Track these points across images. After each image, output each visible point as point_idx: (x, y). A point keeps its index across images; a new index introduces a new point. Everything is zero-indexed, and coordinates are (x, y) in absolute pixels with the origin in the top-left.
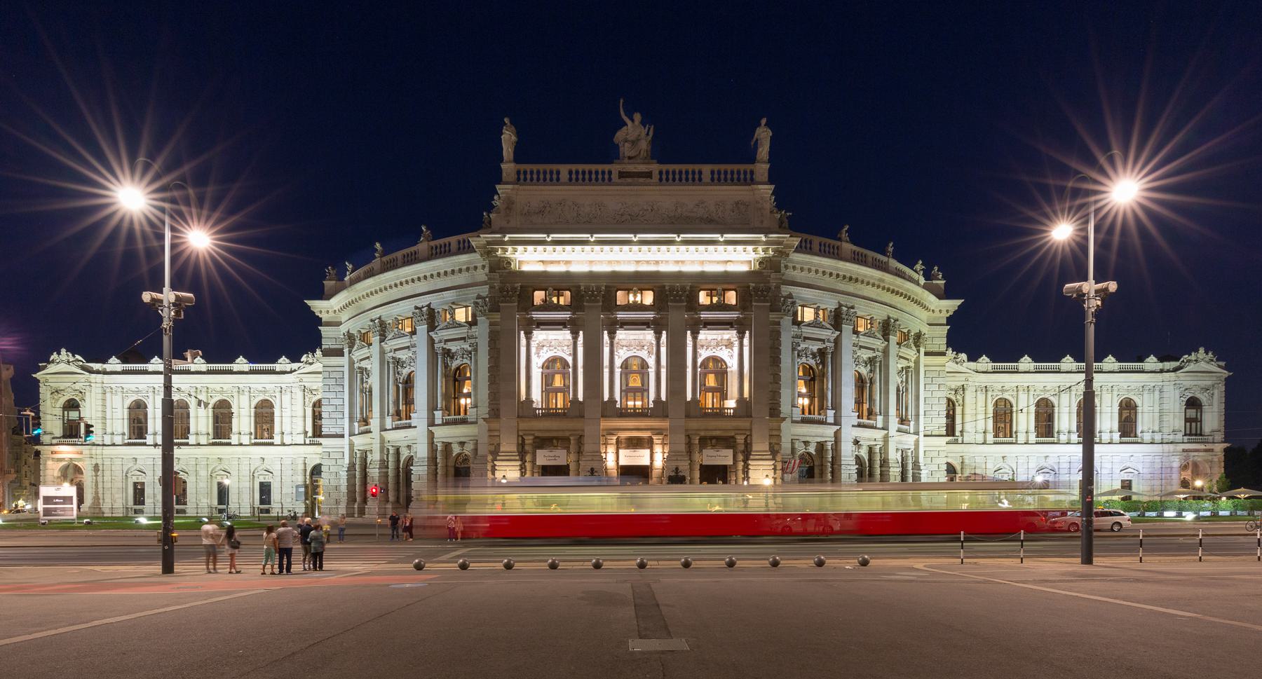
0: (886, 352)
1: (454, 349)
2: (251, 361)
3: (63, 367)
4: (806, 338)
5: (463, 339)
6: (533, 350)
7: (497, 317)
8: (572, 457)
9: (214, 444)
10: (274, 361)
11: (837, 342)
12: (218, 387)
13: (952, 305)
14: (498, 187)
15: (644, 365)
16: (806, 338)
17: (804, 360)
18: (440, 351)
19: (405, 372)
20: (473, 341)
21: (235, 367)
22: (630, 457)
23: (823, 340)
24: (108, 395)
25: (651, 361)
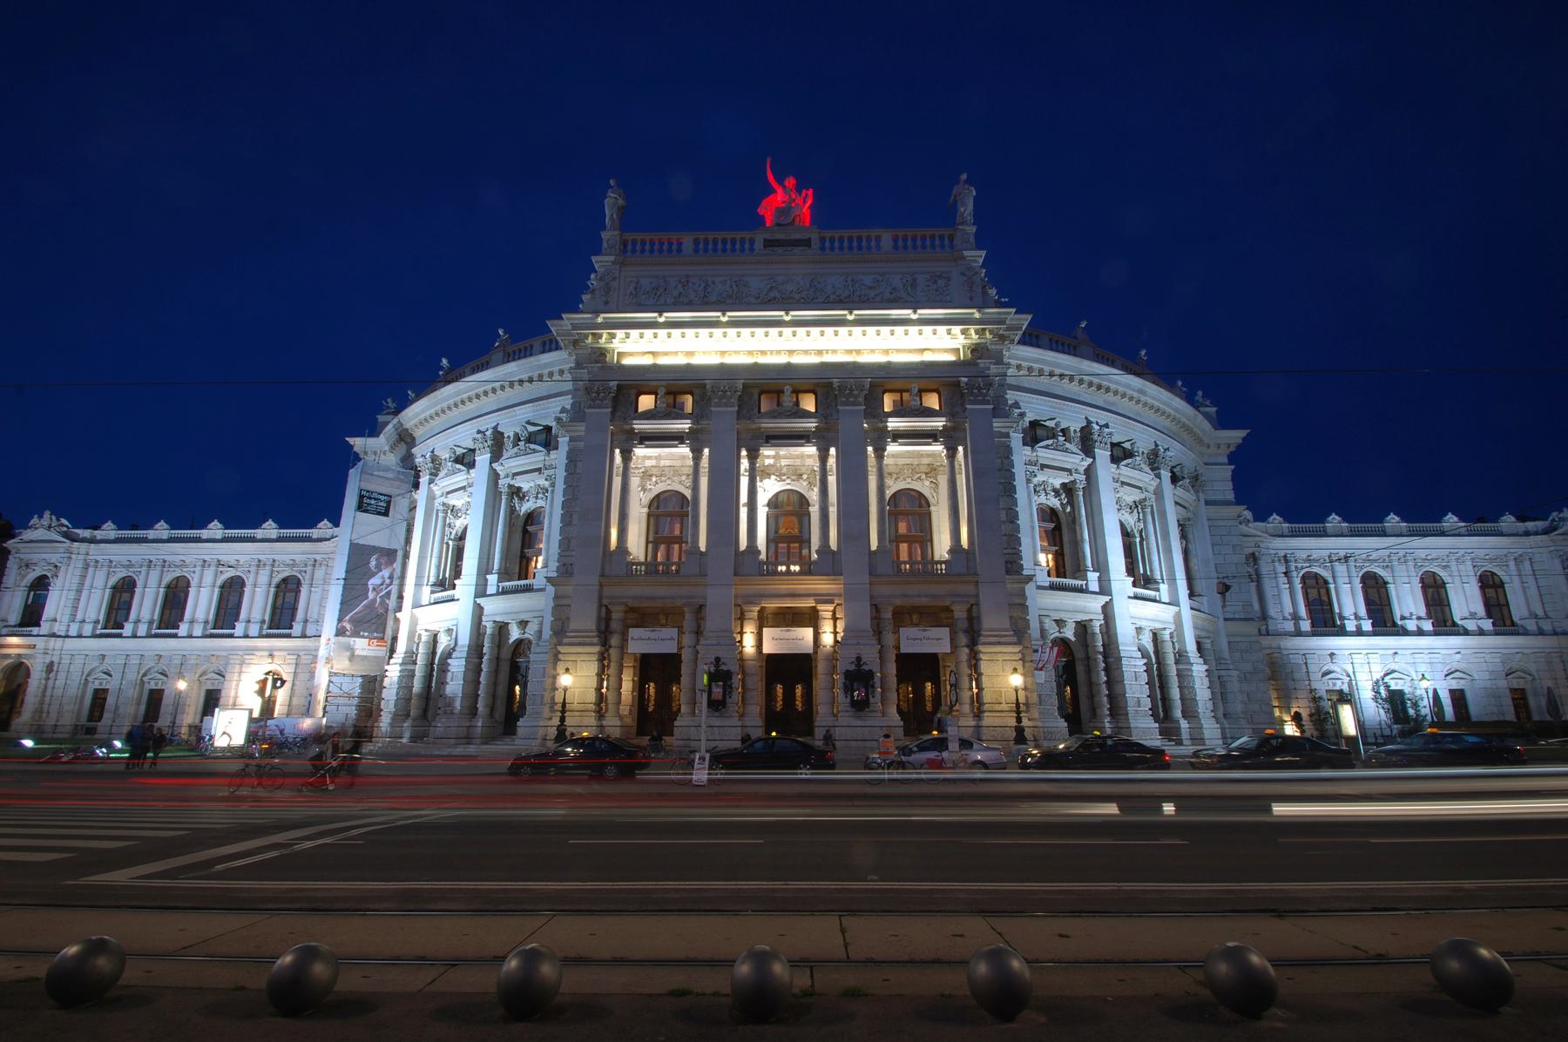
1: (525, 486)
3: (40, 534)
4: (1043, 467)
5: (539, 470)
6: (635, 482)
7: (581, 429)
8: (687, 640)
9: (212, 636)
10: (313, 525)
11: (1089, 472)
14: (594, 259)
15: (803, 501)
16: (1043, 467)
17: (1042, 499)
18: (504, 490)
19: (459, 524)
20: (551, 472)
22: (774, 641)
23: (1069, 471)
24: (91, 570)
25: (814, 496)
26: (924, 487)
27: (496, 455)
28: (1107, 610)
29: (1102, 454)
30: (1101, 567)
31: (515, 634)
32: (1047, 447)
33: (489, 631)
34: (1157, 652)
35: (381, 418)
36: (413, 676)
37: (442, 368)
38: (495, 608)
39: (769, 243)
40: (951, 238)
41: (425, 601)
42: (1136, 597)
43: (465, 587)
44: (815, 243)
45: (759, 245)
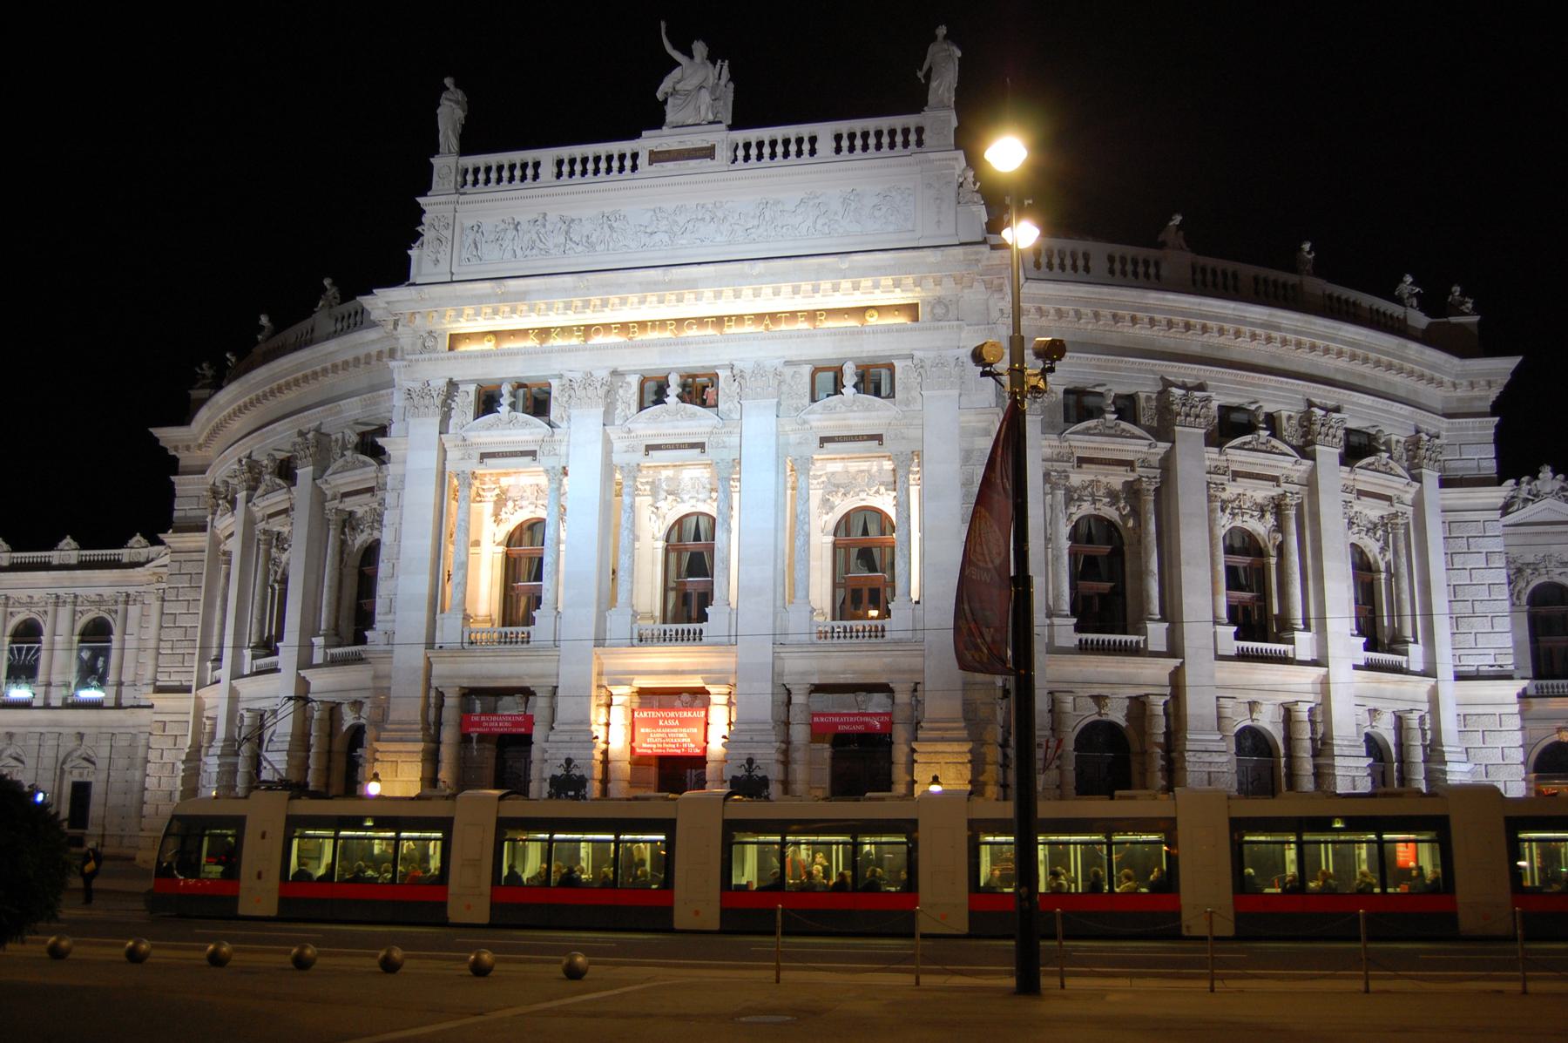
0: (1311, 483)
1: (360, 512)
2: (83, 546)
10: (121, 544)
11: (1167, 465)
12: (23, 595)
13: (1503, 367)
17: (1087, 508)
21: (55, 556)
23: (1129, 464)
26: (885, 502)
27: (321, 471)
28: (1177, 681)
29: (1190, 436)
30: (1171, 614)
31: (349, 719)
32: (1086, 432)
33: (316, 715)
34: (1289, 738)
35: (195, 394)
36: (235, 771)
37: (262, 328)
38: (322, 682)
39: (656, 157)
40: (920, 131)
41: (247, 671)
42: (1243, 656)
43: (287, 654)
44: (723, 154)
45: (643, 160)
